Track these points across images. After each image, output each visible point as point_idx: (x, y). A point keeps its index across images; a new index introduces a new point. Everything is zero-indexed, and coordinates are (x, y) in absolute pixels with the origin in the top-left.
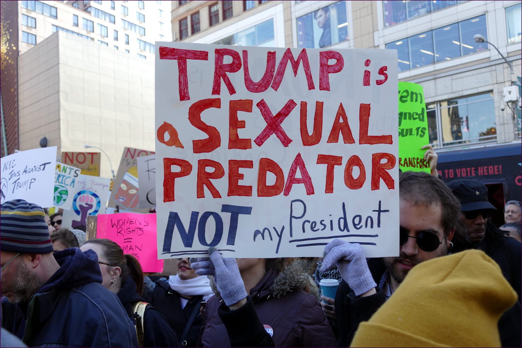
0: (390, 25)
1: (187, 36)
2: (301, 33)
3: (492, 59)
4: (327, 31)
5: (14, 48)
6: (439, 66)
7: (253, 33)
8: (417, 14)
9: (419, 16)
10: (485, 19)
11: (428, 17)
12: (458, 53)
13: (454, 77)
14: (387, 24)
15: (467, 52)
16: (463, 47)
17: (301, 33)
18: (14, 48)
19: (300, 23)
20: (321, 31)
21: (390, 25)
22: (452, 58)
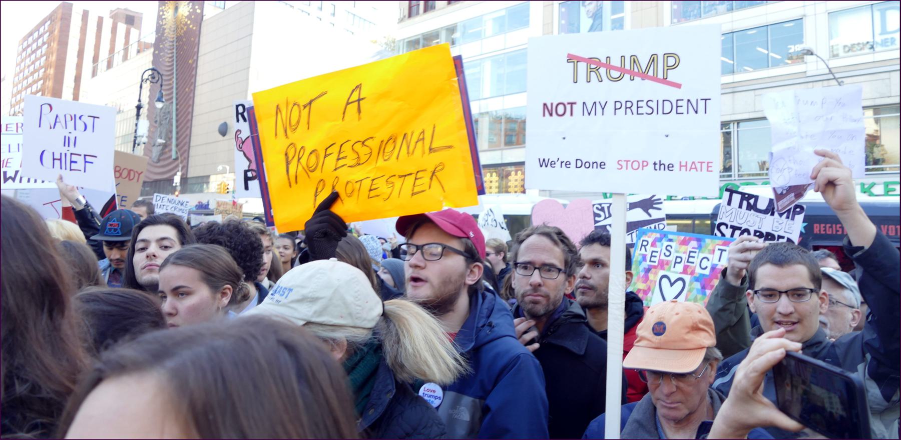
0: (679, 21)
1: (418, 13)
2: (563, 22)
3: (809, 74)
4: (597, 22)
5: (199, 11)
6: (738, 77)
7: (502, 18)
8: (714, 12)
9: (717, 14)
10: (802, 25)
11: (729, 16)
12: (765, 63)
13: (757, 92)
14: (675, 21)
15: (777, 63)
16: (772, 57)
17: (563, 22)
18: (199, 11)
19: (563, 10)
20: (590, 21)
21: (679, 21)
22: (756, 68)
